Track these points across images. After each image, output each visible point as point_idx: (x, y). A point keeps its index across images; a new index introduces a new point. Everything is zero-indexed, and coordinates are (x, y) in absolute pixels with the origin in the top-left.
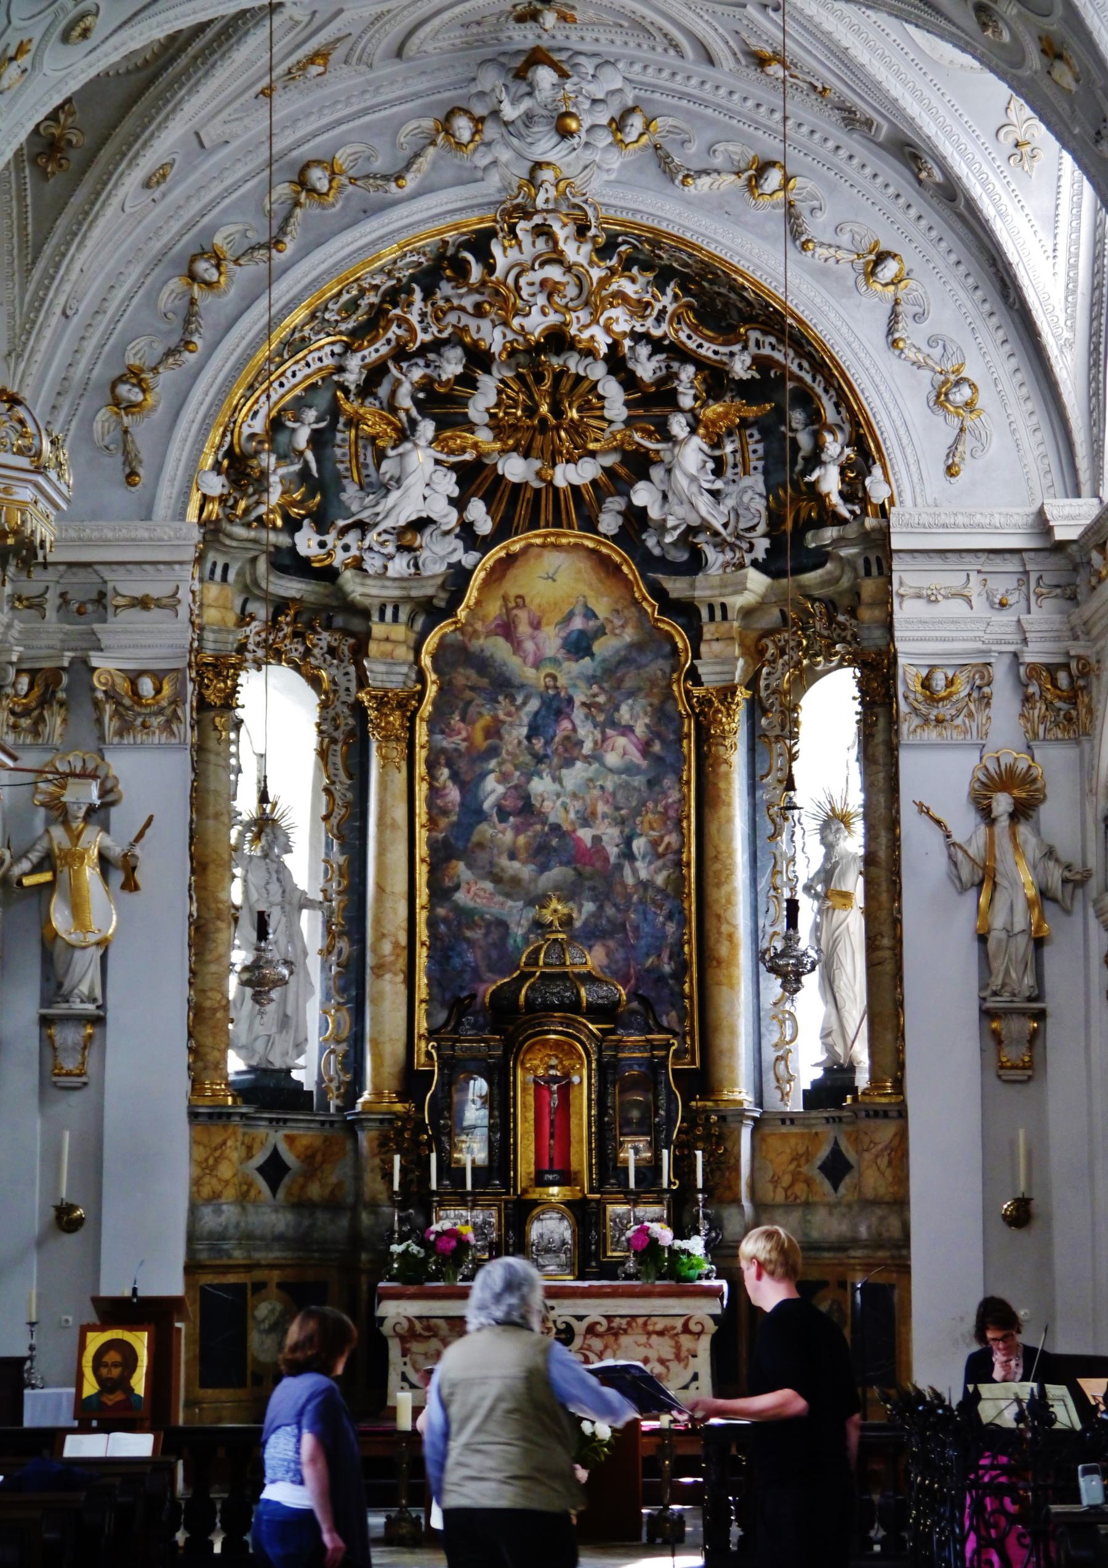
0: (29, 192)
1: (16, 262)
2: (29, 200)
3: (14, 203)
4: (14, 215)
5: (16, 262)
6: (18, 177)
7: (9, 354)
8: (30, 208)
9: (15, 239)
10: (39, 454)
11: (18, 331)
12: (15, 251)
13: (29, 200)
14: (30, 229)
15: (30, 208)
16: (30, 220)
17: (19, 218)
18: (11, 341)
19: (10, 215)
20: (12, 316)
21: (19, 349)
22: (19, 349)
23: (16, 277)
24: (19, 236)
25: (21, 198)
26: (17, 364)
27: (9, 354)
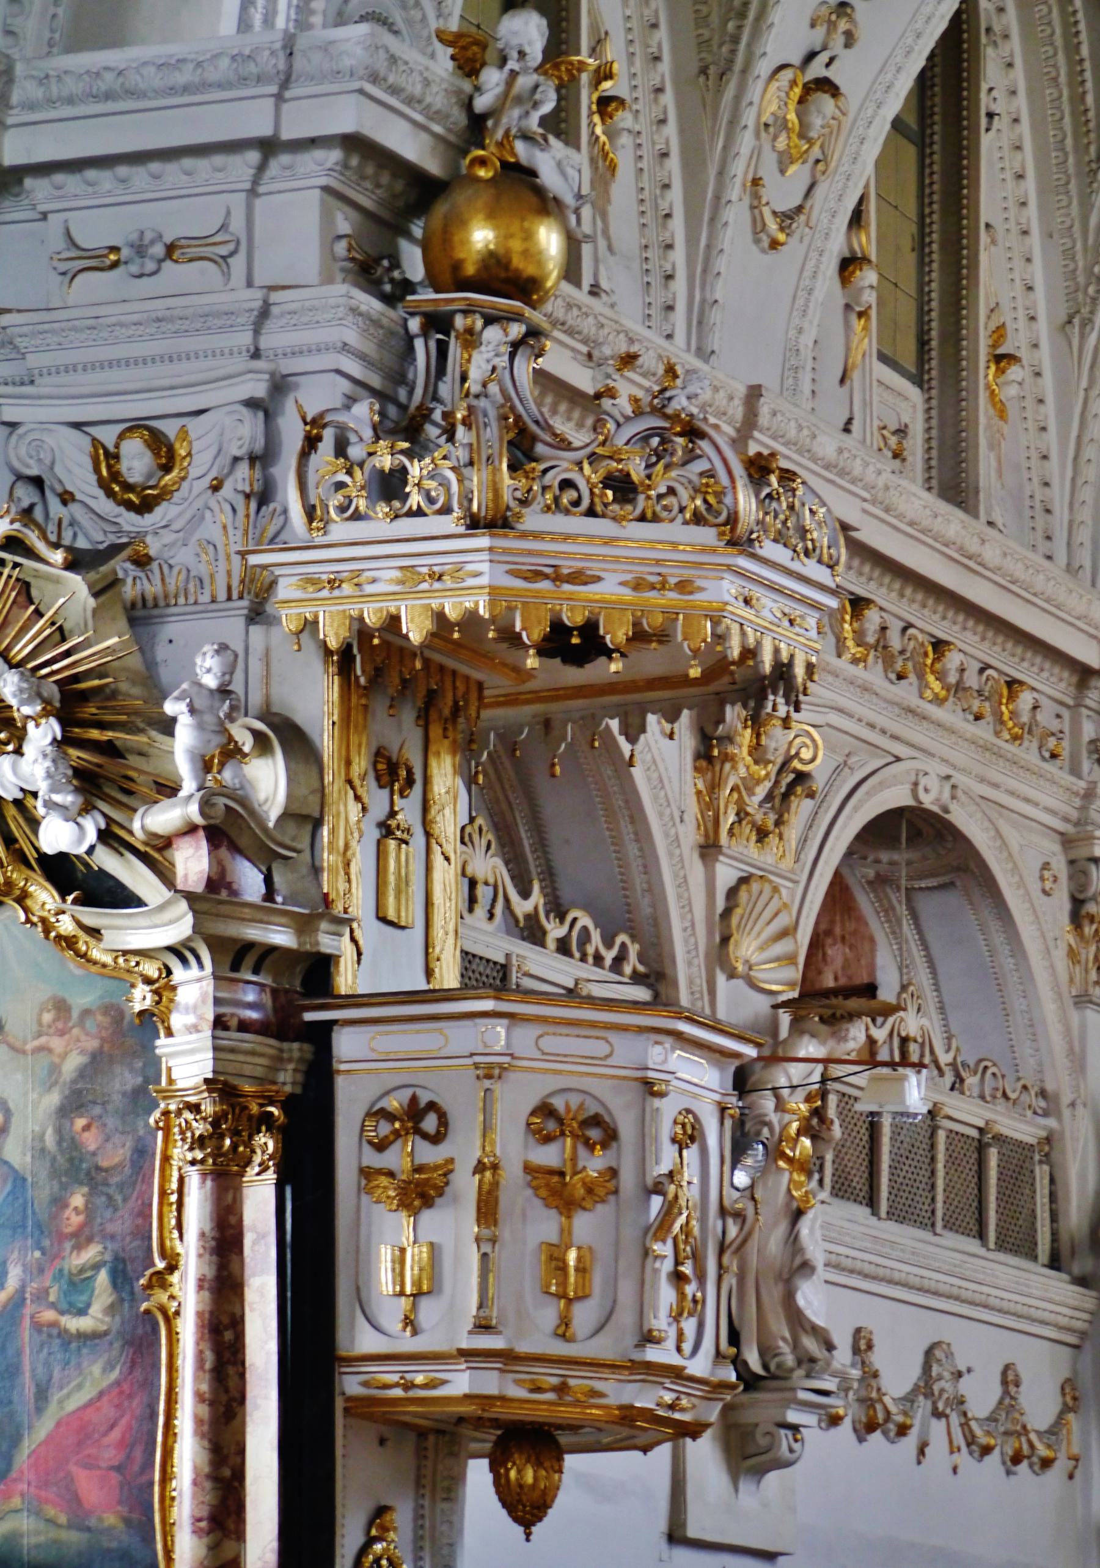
0: (1083, 37)
1: (1071, 160)
2: (1085, 51)
3: (1061, 58)
4: (1063, 79)
5: (1071, 160)
6: (1063, 12)
7: (1069, 322)
8: (1087, 65)
9: (1067, 120)
10: (733, 519)
11: (1081, 279)
12: (1069, 142)
13: (1085, 51)
14: (1090, 99)
15: (1087, 65)
16: (1089, 85)
17: (1070, 85)
18: (1071, 295)
19: (1055, 80)
20: (1069, 254)
21: (1085, 311)
22: (1085, 311)
23: (1073, 186)
24: (1073, 114)
25: (1071, 49)
26: (1083, 337)
27: (1069, 322)
